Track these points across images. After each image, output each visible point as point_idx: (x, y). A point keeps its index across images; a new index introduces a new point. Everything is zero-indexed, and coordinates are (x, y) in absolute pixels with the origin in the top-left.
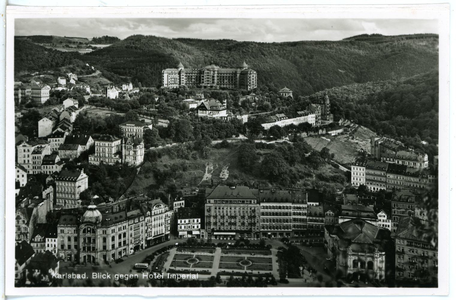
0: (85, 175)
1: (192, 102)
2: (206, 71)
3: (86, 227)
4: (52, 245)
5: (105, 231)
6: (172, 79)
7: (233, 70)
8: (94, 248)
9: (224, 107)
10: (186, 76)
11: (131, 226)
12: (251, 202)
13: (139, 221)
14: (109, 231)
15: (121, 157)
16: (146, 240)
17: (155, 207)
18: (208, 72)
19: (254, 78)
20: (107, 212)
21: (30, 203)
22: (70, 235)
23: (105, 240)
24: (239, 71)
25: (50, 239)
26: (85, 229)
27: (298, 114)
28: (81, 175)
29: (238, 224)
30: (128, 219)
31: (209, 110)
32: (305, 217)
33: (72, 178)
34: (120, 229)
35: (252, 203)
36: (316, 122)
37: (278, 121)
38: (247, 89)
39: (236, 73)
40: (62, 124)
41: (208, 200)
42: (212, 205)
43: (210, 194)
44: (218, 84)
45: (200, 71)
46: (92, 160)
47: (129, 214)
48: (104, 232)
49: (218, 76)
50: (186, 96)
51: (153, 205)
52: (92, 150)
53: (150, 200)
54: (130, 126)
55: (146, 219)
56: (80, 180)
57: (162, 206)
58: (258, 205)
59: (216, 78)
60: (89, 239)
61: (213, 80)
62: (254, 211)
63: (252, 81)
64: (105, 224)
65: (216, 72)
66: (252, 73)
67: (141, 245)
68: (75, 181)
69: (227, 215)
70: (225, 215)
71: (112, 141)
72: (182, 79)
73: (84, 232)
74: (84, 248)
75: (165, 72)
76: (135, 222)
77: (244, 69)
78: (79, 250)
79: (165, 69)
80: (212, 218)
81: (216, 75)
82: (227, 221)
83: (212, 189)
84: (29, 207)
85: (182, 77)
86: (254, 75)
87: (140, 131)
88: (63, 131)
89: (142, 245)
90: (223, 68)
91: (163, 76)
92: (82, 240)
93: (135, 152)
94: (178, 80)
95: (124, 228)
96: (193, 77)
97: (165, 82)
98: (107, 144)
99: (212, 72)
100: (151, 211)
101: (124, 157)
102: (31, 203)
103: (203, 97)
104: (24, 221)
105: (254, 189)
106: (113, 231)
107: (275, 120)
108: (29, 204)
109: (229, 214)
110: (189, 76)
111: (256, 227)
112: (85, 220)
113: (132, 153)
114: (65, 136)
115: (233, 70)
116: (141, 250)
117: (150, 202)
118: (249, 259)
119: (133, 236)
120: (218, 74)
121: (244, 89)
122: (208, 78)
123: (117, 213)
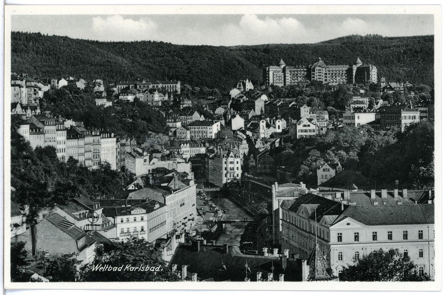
10: (290, 74)
18: (320, 68)
19: (375, 73)
24: (355, 68)
72: (287, 78)
75: (270, 69)
85: (287, 75)
94: (283, 79)
96: (299, 75)
122: (320, 75)
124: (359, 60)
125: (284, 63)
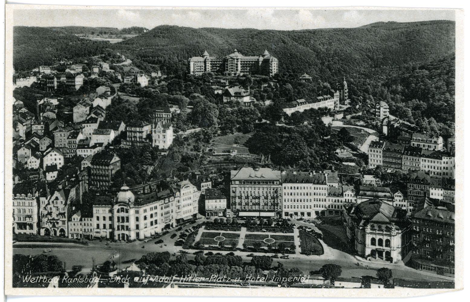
0: (117, 159)
1: (217, 88)
2: (230, 59)
3: (120, 207)
4: (88, 224)
5: (138, 211)
6: (198, 67)
7: (255, 58)
8: (127, 227)
9: (247, 94)
10: (211, 64)
11: (161, 206)
12: (273, 183)
13: (169, 201)
14: (141, 210)
15: (151, 140)
16: (176, 220)
17: (183, 188)
19: (276, 65)
20: (139, 193)
21: (67, 184)
22: (104, 215)
23: (137, 219)
24: (261, 59)
25: (86, 219)
26: (119, 210)
27: (318, 100)
28: (114, 158)
29: (262, 204)
30: (159, 199)
31: (233, 96)
32: (324, 197)
33: (106, 161)
34: (151, 209)
35: (275, 184)
36: (335, 107)
37: (299, 105)
38: (269, 76)
39: (258, 62)
40: (96, 110)
41: (233, 182)
42: (237, 186)
43: (235, 176)
44: (241, 72)
45: (225, 59)
46: (124, 145)
47: (159, 195)
48: (137, 212)
49: (241, 64)
50: (212, 83)
51: (182, 187)
52: (123, 135)
53: (179, 182)
54: (160, 112)
55: (176, 199)
56: (113, 163)
57: (191, 186)
58: (280, 186)
59: (239, 66)
60: (123, 218)
61: (237, 67)
62: (276, 192)
63: (273, 68)
64: (138, 203)
65: (239, 60)
66: (273, 60)
67: (171, 224)
68: (108, 165)
69: (251, 195)
70: (249, 195)
71: (143, 127)
72: (207, 67)
73: (118, 211)
74: (118, 226)
75: (191, 60)
76: (166, 202)
77: (266, 56)
78: (113, 229)
79: (191, 57)
80: (237, 198)
81: (239, 63)
82: (251, 201)
83: (237, 171)
84: (67, 188)
85: (207, 65)
86: (276, 63)
87: (169, 117)
88: (96, 117)
89: (172, 223)
90: (246, 56)
91: (190, 64)
92: (116, 220)
93: (164, 137)
94: (204, 68)
95: (156, 208)
97: (192, 69)
98: (138, 129)
99: (235, 60)
100: (180, 192)
101: (154, 141)
102: (68, 185)
103: (227, 84)
104: (62, 202)
105: (276, 171)
106: (145, 211)
107: (296, 105)
108: (66, 186)
109: (253, 195)
110: (214, 64)
111: (279, 207)
112: (119, 200)
113: (161, 136)
114: (98, 122)
115: (255, 58)
116: (171, 228)
117: (179, 183)
118: (272, 236)
119: (164, 215)
120: (241, 62)
121: (266, 75)
123: (148, 193)
124: (266, 52)
125: (208, 54)
